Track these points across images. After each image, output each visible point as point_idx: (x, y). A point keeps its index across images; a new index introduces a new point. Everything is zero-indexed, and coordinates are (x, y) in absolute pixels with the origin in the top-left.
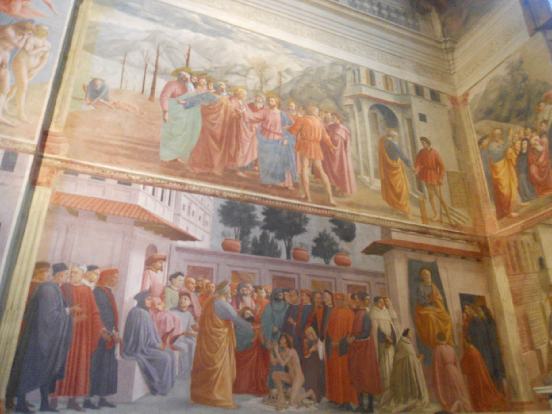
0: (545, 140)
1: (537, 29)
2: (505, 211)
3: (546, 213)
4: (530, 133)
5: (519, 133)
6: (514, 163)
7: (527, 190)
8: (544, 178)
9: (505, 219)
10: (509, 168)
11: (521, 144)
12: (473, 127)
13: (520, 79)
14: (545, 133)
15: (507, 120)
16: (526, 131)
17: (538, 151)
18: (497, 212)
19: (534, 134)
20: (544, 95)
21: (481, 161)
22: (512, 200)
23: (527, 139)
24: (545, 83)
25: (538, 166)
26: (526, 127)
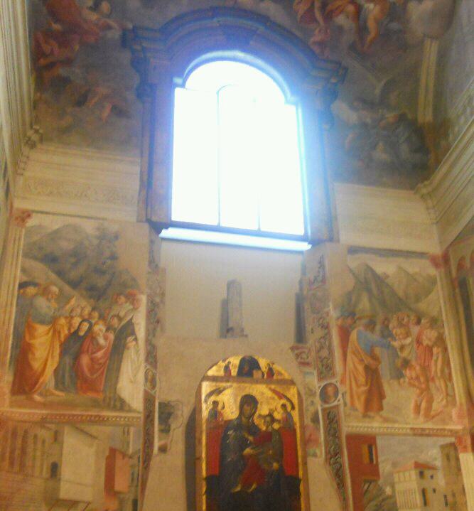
0: (112, 336)
1: (149, 221)
3: (82, 416)
4: (96, 319)
5: (83, 309)
6: (63, 339)
7: (67, 375)
8: (95, 376)
11: (80, 324)
13: (107, 253)
14: (114, 330)
15: (75, 285)
16: (93, 313)
17: (98, 344)
19: (101, 323)
20: (129, 290)
24: (134, 279)
25: (92, 359)
26: (94, 309)
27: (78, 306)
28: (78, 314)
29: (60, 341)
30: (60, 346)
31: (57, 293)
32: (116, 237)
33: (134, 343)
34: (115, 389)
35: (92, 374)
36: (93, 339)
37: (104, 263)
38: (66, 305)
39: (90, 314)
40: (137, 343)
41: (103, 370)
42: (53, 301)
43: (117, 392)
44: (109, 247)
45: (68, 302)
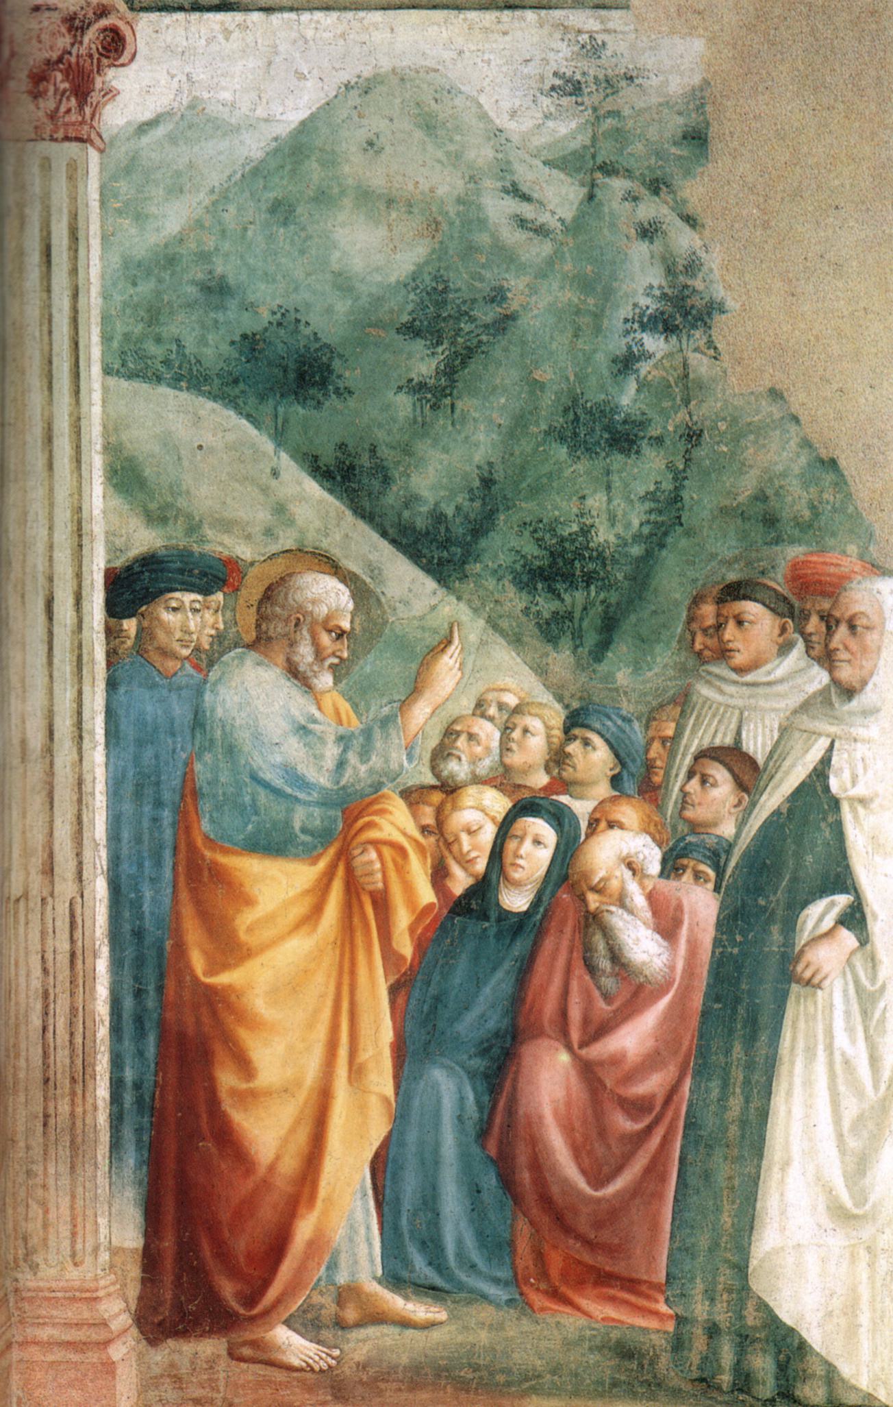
2: (228, 1289)
4: (603, 790)
6: (406, 948)
9: (210, 1347)
10: (347, 971)
11: (505, 828)
12: (95, 411)
14: (717, 856)
16: (574, 748)
17: (616, 956)
18: (150, 1260)
19: (629, 813)
21: (97, 757)
22: (304, 1230)
23: (560, 818)
25: (588, 1071)
26: (575, 721)
27: (480, 707)
28: (485, 766)
29: (389, 954)
30: (394, 990)
31: (346, 625)
32: (697, 138)
33: (847, 939)
34: (742, 1269)
35: (598, 1181)
36: (592, 922)
37: (626, 363)
38: (405, 704)
39: (558, 758)
40: (864, 940)
41: (666, 1141)
42: (325, 680)
43: (754, 1284)
44: (648, 232)
45: (416, 689)
